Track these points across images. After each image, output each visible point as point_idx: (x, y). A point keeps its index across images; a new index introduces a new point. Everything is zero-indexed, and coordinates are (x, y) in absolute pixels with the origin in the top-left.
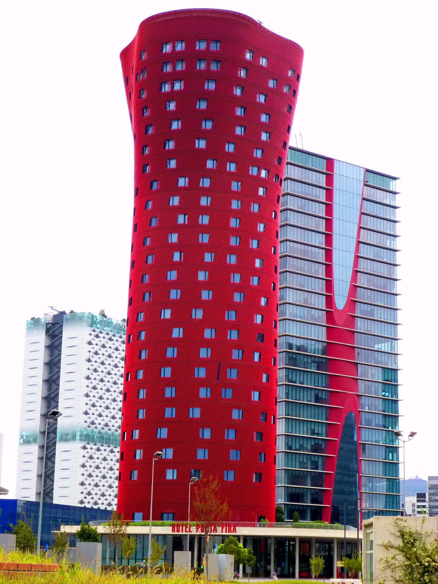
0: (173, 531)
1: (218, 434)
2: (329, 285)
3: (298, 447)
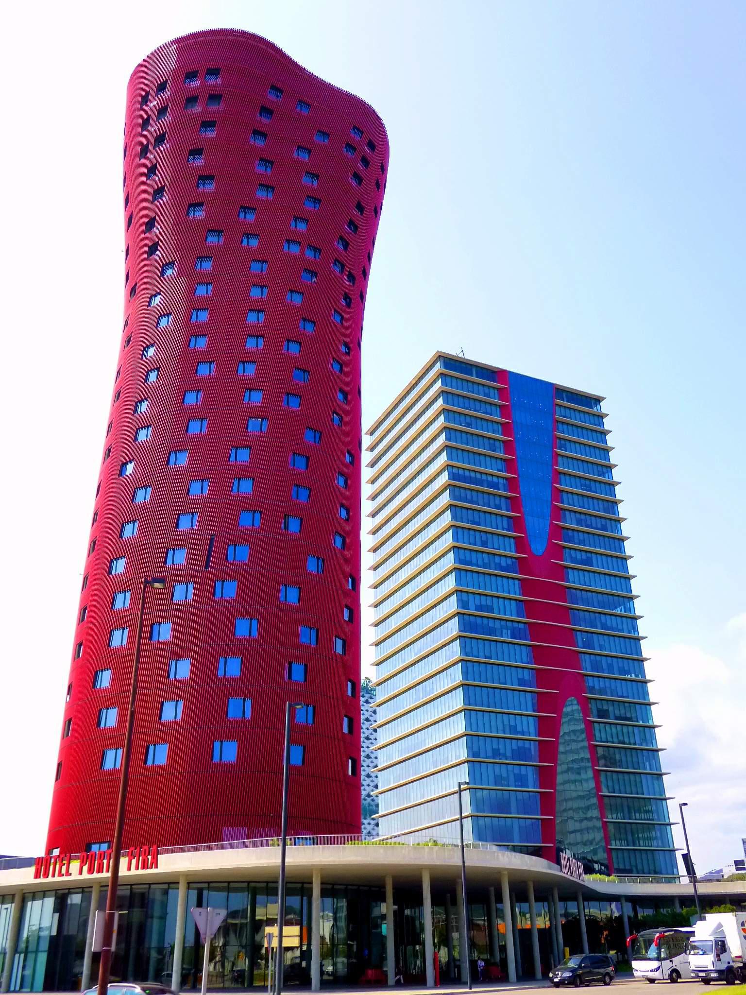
0: (37, 876)
1: (205, 669)
2: (517, 524)
3: (490, 753)
